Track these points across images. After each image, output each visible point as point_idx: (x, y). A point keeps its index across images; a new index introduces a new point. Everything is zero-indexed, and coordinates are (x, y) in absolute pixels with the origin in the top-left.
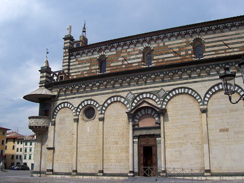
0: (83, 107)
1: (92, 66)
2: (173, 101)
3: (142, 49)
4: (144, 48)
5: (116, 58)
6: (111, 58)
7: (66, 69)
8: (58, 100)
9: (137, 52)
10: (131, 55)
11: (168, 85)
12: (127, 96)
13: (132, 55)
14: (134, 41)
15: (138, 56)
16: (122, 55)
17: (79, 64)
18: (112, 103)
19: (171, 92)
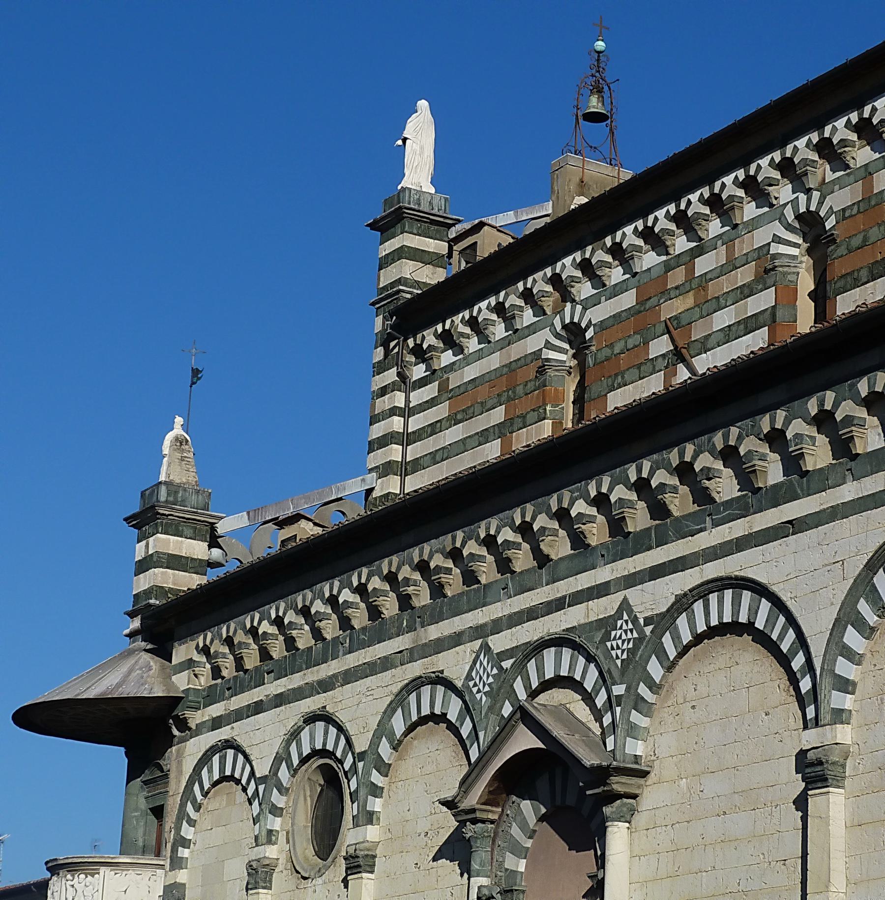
1: (518, 422)
12: (469, 677)
17: (453, 420)
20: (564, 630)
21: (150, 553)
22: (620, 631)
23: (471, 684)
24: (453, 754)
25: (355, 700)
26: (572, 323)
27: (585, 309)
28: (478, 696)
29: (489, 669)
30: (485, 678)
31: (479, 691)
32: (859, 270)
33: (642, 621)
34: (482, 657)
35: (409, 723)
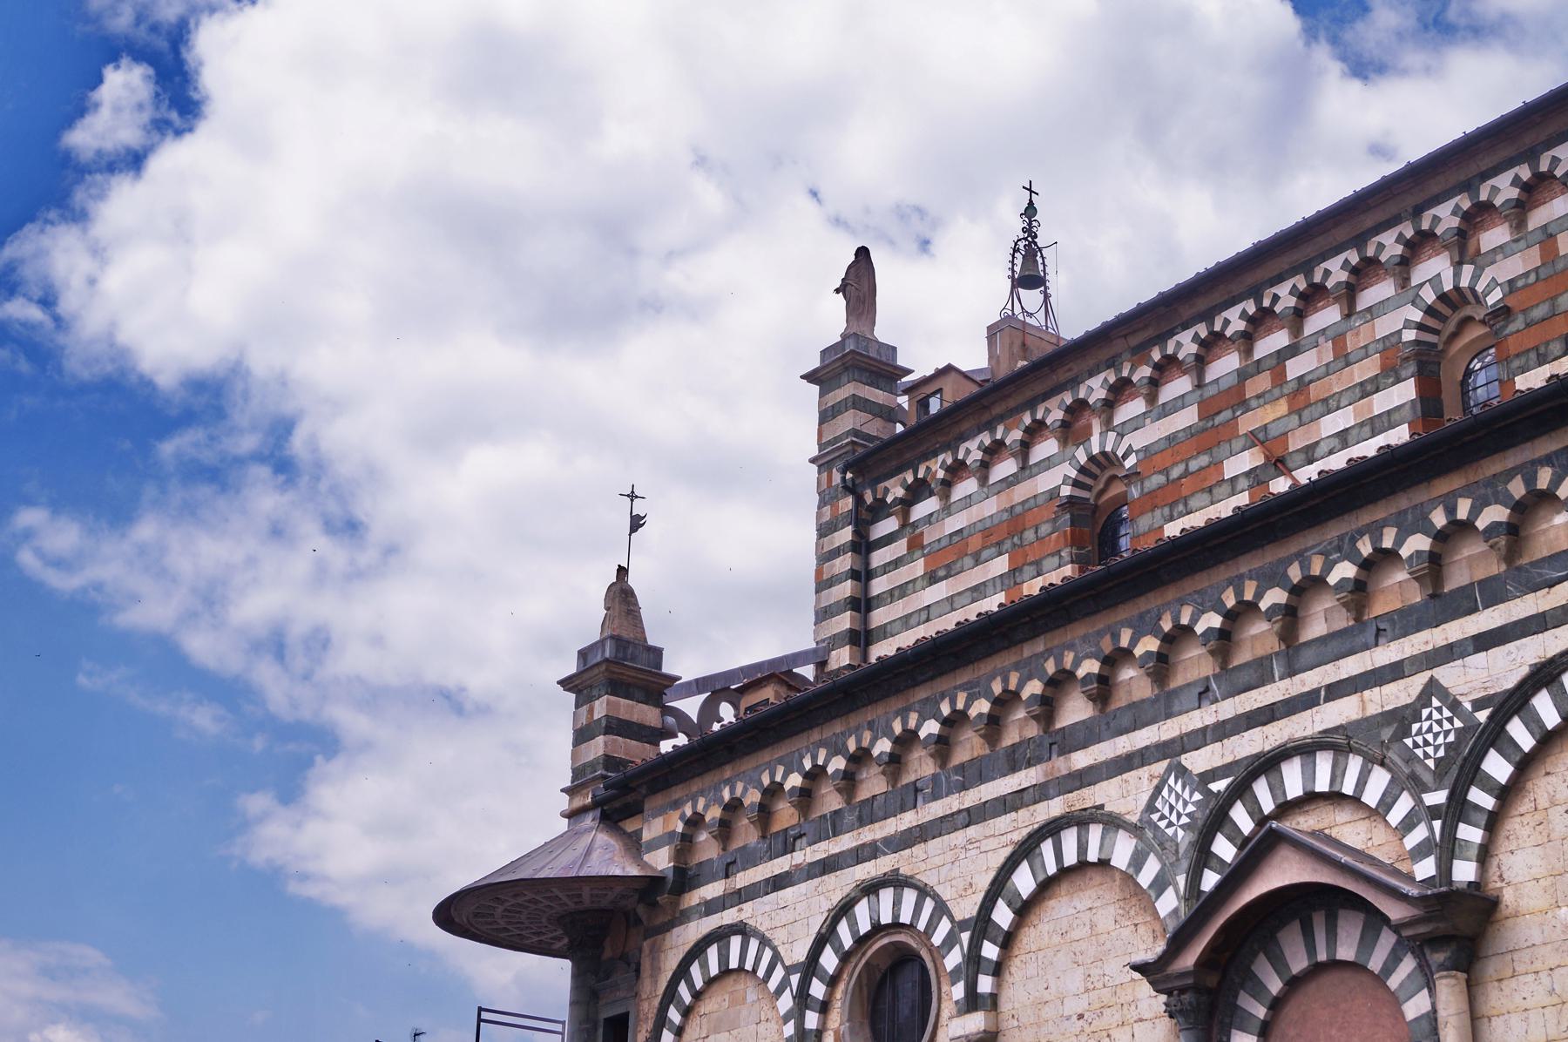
0: (845, 957)
2: (1553, 804)
3: (1408, 324)
4: (1430, 311)
5: (1204, 460)
6: (1165, 471)
7: (834, 642)
8: (683, 917)
9: (1367, 369)
10: (1320, 408)
11: (1485, 641)
12: (1151, 807)
13: (1329, 405)
14: (1329, 265)
15: (1382, 402)
16: (1248, 422)
17: (932, 578)
18: (1046, 887)
19: (1515, 702)
20: (1320, 732)
21: (596, 718)
22: (1428, 723)
23: (1155, 817)
24: (1121, 912)
25: (949, 856)
26: (1103, 453)
27: (1121, 436)
28: (1170, 831)
29: (1186, 795)
30: (1180, 806)
31: (1170, 824)
32: (1547, 343)
33: (1468, 706)
34: (1171, 781)
35: (1041, 877)
